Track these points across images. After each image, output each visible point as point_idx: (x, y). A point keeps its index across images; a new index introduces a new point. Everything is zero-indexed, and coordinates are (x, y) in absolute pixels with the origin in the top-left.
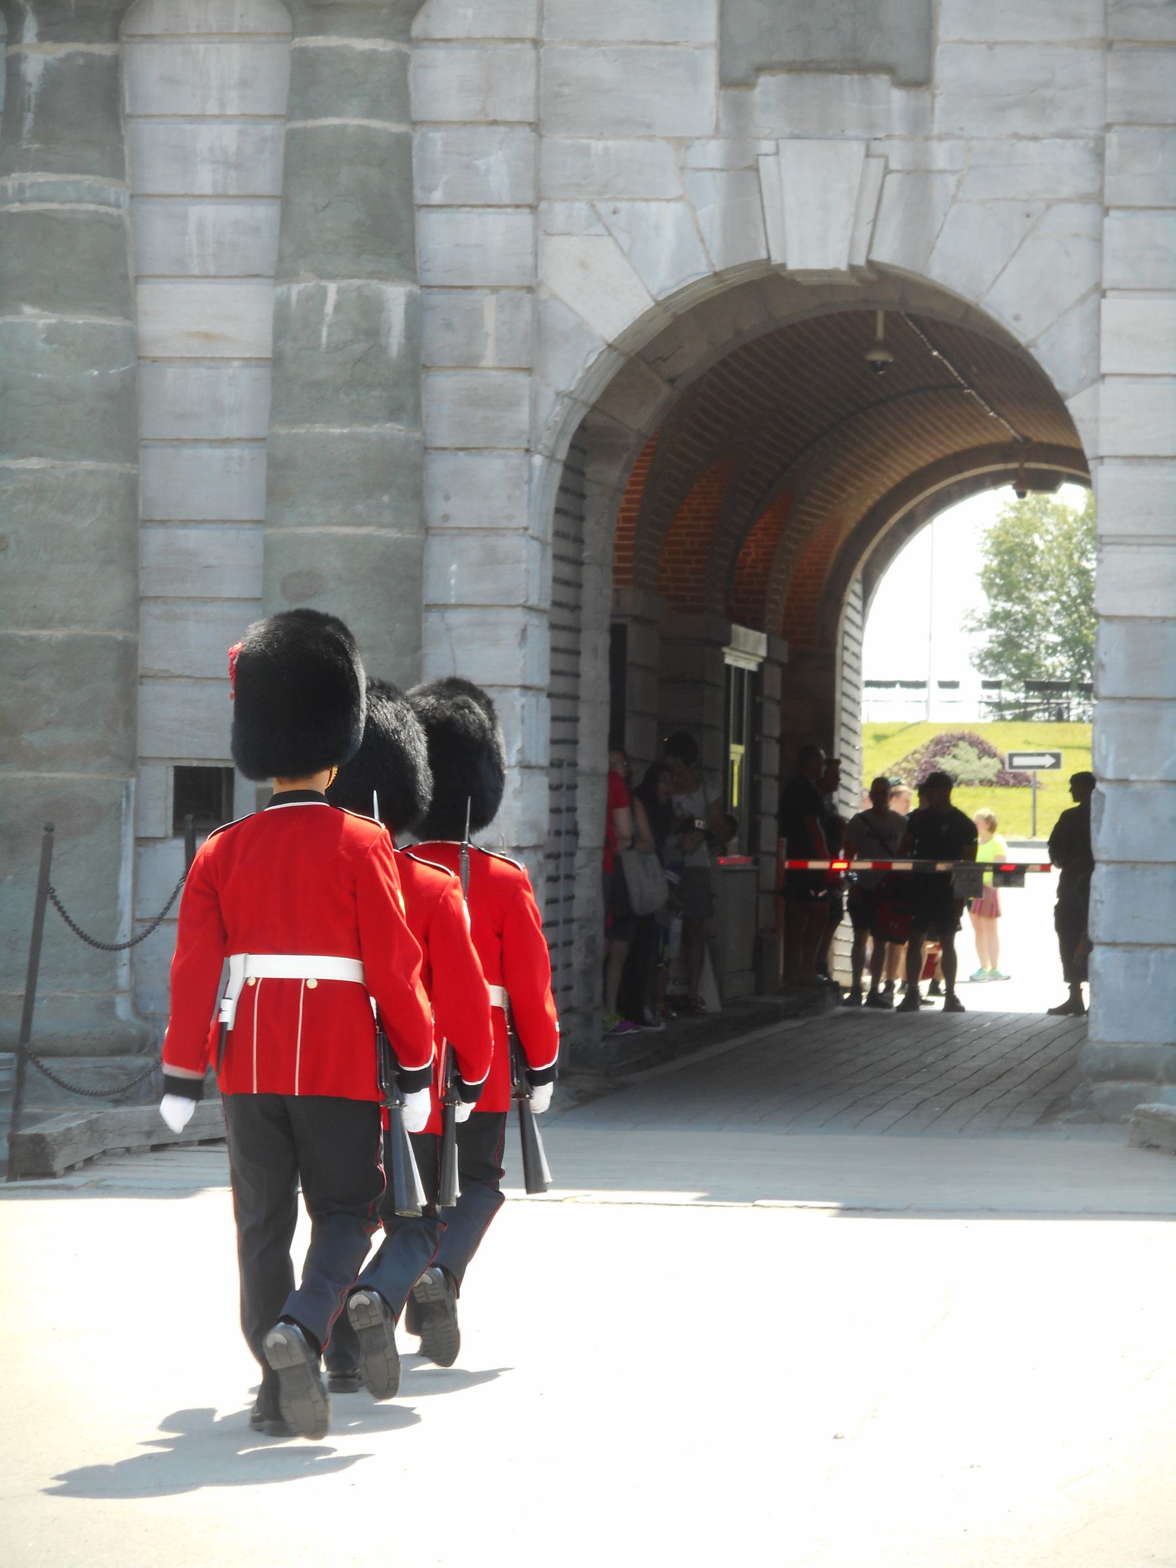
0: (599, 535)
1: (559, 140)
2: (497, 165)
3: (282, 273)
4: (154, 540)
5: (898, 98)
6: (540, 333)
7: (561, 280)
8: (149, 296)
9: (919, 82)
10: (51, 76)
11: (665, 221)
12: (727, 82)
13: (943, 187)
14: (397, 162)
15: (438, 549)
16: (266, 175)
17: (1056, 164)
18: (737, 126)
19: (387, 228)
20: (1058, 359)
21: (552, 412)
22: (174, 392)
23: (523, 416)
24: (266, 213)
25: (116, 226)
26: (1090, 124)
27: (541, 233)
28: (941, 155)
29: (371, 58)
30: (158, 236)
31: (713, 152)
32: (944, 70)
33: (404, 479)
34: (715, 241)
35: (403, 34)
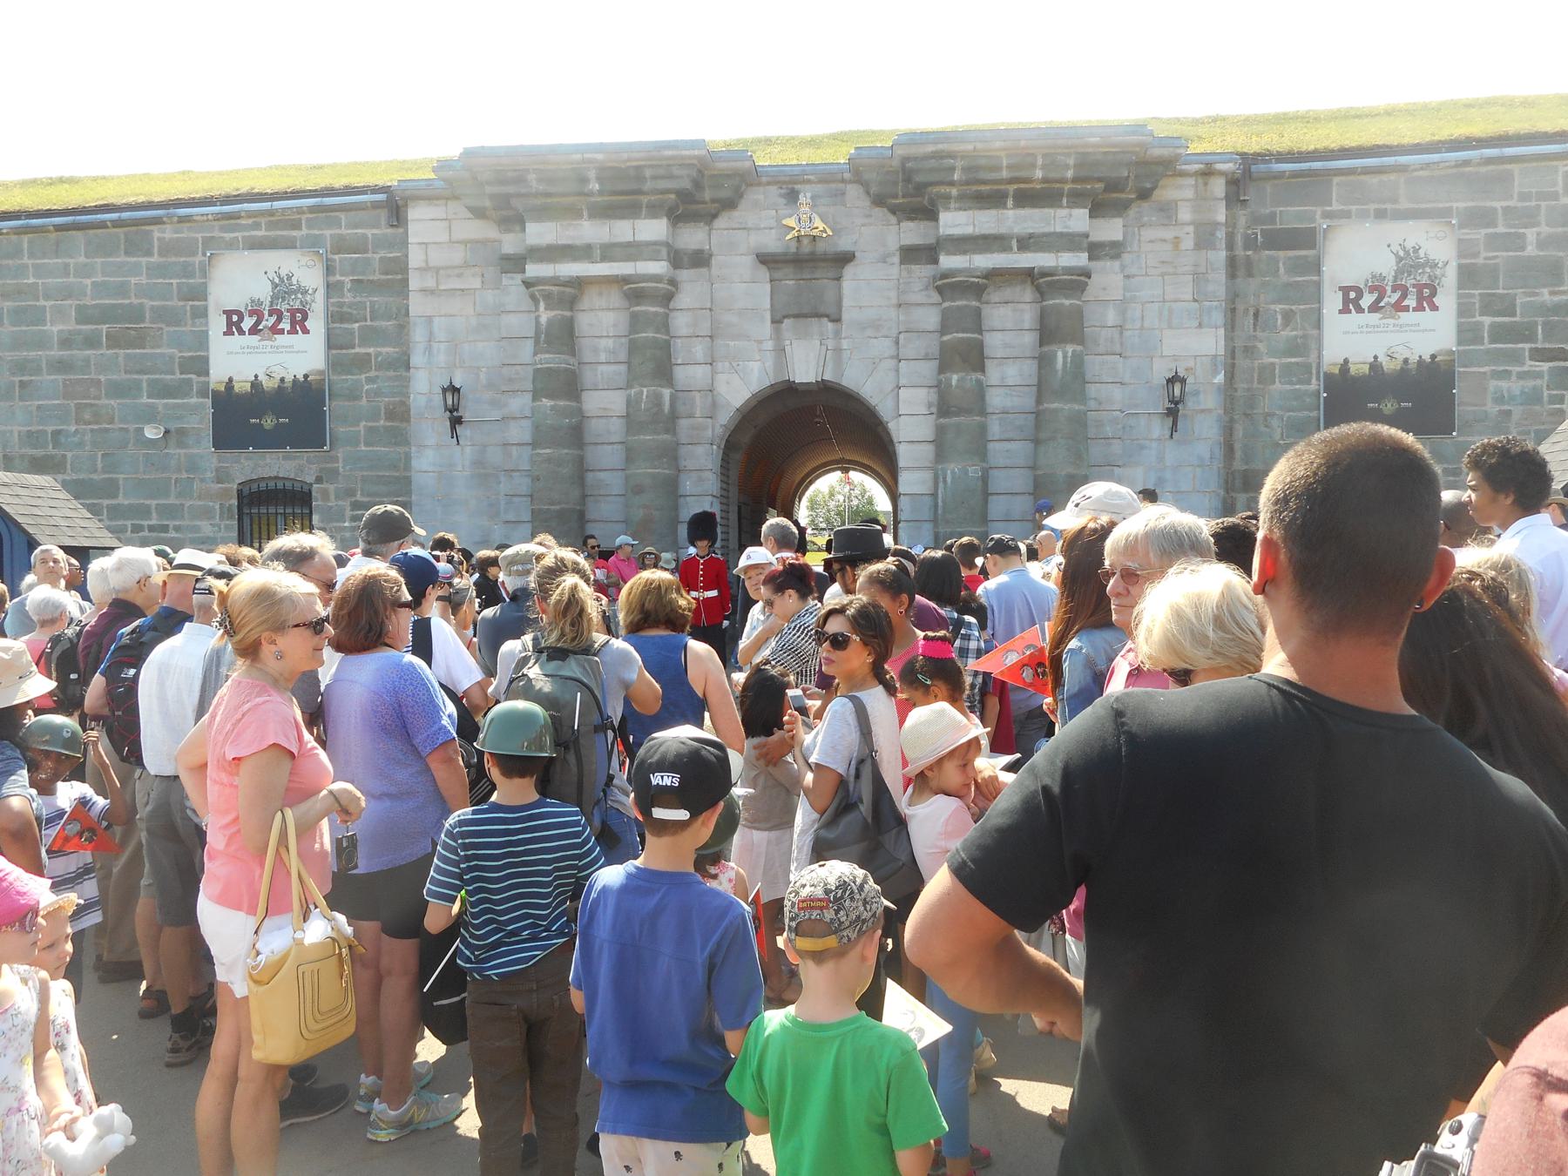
0: (734, 474)
1: (719, 342)
2: (699, 350)
3: (629, 386)
4: (590, 476)
5: (830, 325)
6: (714, 404)
7: (722, 389)
8: (585, 396)
9: (837, 320)
10: (550, 322)
11: (755, 367)
12: (773, 322)
13: (846, 355)
14: (666, 347)
15: (683, 476)
16: (623, 356)
17: (883, 346)
18: (777, 336)
19: (663, 370)
20: (884, 409)
21: (719, 430)
22: (595, 427)
23: (710, 432)
24: (623, 368)
25: (573, 372)
26: (894, 332)
27: (714, 373)
28: (845, 344)
29: (656, 314)
30: (588, 376)
31: (769, 345)
32: (845, 316)
33: (671, 454)
34: (771, 374)
35: (667, 306)
